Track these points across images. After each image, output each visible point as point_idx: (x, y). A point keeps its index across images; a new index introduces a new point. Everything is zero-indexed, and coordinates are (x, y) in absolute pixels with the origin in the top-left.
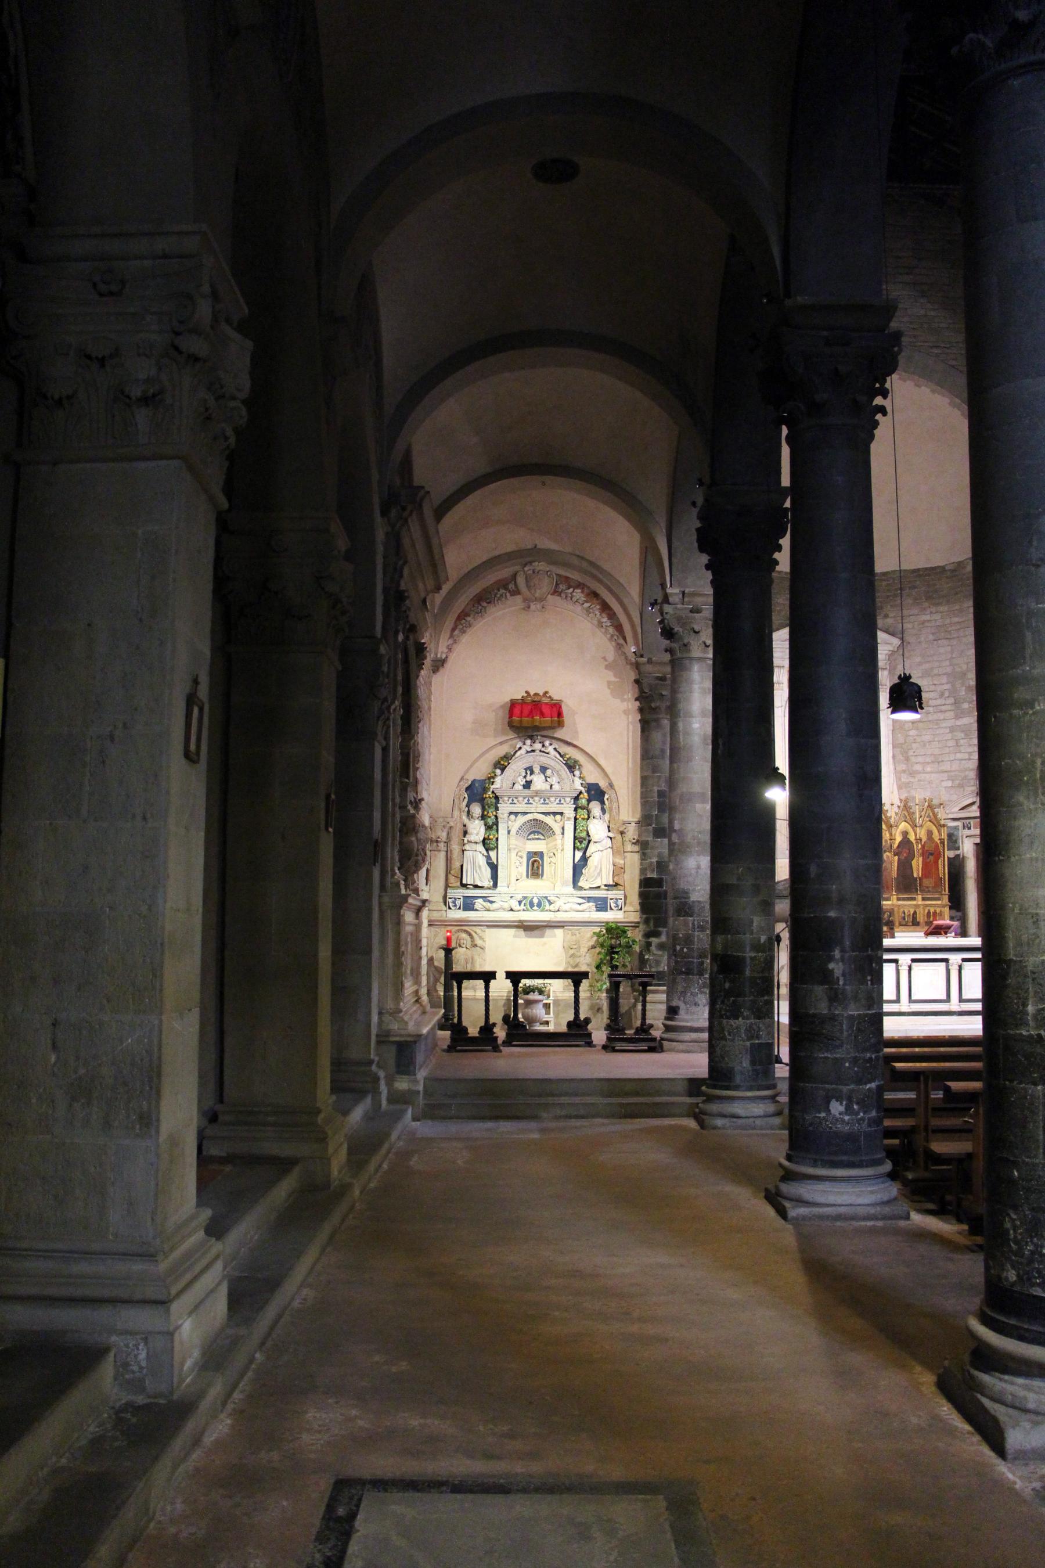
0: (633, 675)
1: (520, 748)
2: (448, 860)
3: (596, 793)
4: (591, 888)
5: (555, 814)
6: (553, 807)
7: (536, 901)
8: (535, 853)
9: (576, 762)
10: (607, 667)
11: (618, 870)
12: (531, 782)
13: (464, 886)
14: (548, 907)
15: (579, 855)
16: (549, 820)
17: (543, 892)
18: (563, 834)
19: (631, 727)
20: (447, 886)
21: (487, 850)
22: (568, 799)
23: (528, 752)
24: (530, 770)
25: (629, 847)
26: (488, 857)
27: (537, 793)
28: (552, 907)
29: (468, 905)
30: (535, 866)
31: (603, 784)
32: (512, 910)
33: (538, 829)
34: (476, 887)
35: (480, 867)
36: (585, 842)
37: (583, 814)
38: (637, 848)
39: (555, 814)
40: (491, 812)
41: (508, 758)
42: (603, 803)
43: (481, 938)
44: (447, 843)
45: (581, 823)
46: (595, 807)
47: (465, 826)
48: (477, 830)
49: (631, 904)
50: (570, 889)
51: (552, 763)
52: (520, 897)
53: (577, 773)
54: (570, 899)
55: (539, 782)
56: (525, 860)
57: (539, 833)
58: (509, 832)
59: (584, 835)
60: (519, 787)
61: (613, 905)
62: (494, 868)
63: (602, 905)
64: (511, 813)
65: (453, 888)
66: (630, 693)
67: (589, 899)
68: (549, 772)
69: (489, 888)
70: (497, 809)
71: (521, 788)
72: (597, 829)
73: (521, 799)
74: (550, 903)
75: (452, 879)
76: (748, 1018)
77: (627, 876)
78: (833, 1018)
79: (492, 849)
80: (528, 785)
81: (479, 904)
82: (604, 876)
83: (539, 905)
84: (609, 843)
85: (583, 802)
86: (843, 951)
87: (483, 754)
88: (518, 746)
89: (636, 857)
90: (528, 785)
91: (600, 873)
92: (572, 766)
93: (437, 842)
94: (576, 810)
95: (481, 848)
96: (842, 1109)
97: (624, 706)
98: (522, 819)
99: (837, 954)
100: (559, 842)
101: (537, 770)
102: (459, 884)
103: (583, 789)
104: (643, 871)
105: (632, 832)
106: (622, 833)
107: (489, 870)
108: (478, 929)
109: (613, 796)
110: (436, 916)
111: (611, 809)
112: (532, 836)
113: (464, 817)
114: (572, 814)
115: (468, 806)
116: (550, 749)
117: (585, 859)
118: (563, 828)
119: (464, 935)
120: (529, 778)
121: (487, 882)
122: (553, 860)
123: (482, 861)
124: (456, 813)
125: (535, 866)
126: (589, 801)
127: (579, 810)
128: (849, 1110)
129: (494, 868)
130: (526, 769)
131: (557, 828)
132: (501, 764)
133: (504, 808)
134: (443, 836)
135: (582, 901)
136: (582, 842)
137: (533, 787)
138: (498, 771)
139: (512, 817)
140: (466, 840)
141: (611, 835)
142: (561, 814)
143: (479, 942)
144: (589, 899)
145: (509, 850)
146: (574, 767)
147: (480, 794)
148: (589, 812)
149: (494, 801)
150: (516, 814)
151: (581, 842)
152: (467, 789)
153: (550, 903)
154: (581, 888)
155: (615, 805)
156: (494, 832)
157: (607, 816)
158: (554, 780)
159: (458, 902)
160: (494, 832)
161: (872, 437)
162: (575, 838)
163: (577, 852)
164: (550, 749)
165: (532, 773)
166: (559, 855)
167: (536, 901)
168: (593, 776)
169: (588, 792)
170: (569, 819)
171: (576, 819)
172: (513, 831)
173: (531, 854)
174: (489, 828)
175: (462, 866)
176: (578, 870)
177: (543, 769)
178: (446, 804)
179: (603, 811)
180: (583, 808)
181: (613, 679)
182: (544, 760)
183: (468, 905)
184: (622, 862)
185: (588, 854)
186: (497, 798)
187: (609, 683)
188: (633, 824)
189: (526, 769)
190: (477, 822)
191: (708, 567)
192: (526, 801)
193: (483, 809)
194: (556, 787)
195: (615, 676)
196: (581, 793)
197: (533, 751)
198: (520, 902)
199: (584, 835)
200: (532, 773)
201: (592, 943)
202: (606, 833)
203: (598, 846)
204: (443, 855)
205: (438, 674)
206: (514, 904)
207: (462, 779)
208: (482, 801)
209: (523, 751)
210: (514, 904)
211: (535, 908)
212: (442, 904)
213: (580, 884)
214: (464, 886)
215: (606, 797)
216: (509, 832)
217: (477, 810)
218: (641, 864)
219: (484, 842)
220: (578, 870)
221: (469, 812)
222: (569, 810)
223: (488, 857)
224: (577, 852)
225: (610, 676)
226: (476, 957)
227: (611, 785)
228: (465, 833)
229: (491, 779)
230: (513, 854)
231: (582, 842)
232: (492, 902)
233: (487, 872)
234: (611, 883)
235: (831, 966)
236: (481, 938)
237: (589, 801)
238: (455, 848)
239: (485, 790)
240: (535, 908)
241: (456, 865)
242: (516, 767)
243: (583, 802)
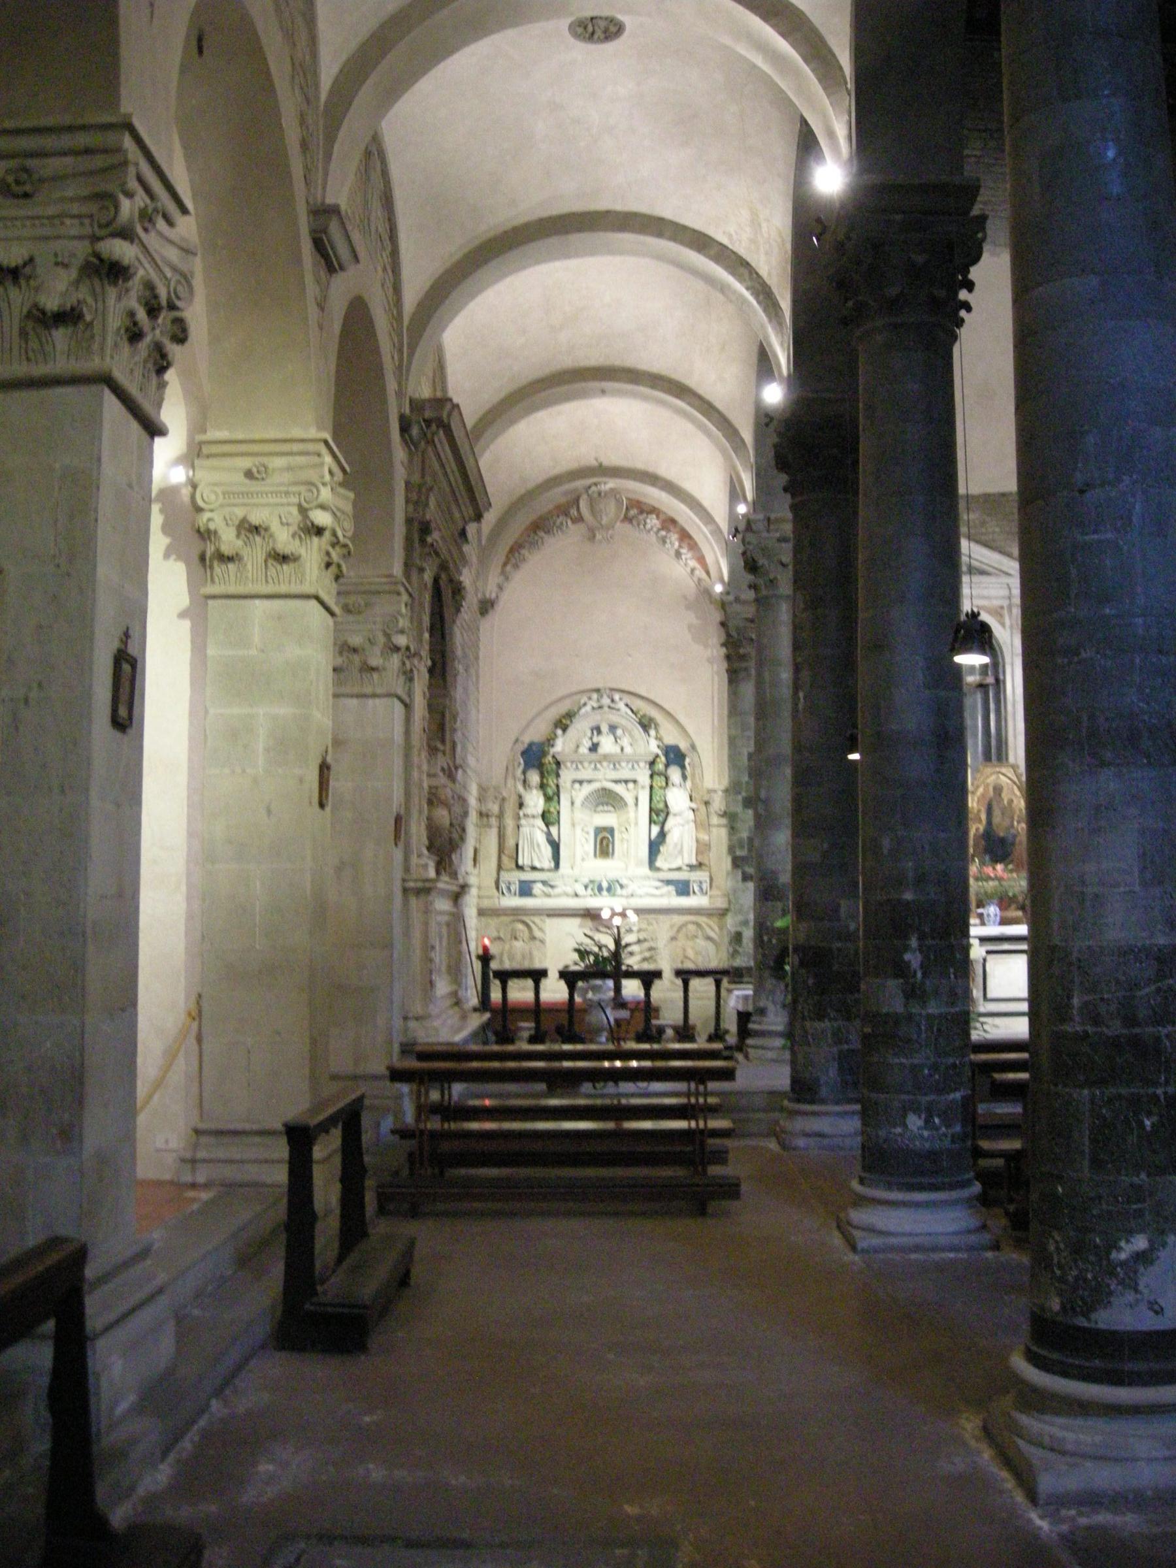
0: (717, 616)
1: (585, 704)
2: (501, 837)
3: (675, 756)
4: (671, 870)
6: (625, 773)
7: (605, 885)
8: (604, 829)
9: (651, 720)
10: (688, 608)
11: (702, 848)
13: (520, 868)
14: (619, 891)
15: (655, 830)
17: (612, 875)
18: (636, 804)
19: (716, 678)
20: (500, 868)
21: (547, 825)
22: (642, 764)
23: (593, 708)
24: (598, 730)
25: (715, 820)
26: (549, 834)
27: (606, 757)
28: (624, 892)
29: (525, 890)
30: (604, 843)
31: (683, 746)
32: (576, 895)
33: (607, 799)
34: (534, 868)
35: (538, 845)
36: (663, 815)
37: (659, 781)
38: (724, 821)
39: (626, 782)
40: (551, 781)
41: (570, 715)
42: (683, 767)
43: (541, 929)
44: (501, 816)
45: (658, 792)
46: (675, 774)
47: (520, 797)
48: (535, 802)
49: (718, 888)
50: (645, 870)
51: (623, 722)
52: (586, 880)
53: (652, 732)
54: (647, 883)
55: (607, 744)
57: (607, 804)
58: (573, 803)
59: (661, 806)
60: (584, 750)
61: (696, 889)
62: (555, 846)
63: (683, 889)
64: (574, 781)
65: (508, 870)
66: (715, 637)
67: (668, 882)
68: (619, 732)
69: (549, 870)
70: (558, 776)
72: (677, 798)
73: (586, 764)
74: (622, 886)
75: (506, 861)
76: (836, 1020)
77: (713, 855)
78: (910, 1017)
79: (553, 824)
80: (594, 748)
81: (538, 888)
82: (686, 855)
83: (609, 889)
84: (691, 815)
85: (660, 766)
86: (921, 938)
87: (539, 714)
88: (582, 702)
89: (723, 833)
90: (594, 748)
91: (681, 852)
92: (646, 724)
93: (488, 816)
94: (651, 776)
95: (540, 823)
96: (920, 1123)
97: (709, 653)
98: (587, 789)
99: (914, 942)
100: (632, 814)
101: (605, 728)
102: (514, 866)
103: (660, 752)
104: (731, 850)
105: (718, 803)
106: (707, 803)
107: (549, 849)
108: (537, 919)
109: (696, 759)
110: (486, 903)
111: (693, 775)
112: (601, 808)
113: (520, 788)
114: (647, 782)
115: (524, 773)
116: (621, 705)
117: (662, 835)
118: (637, 799)
119: (520, 926)
120: (595, 740)
121: (546, 861)
122: (625, 836)
123: (541, 838)
124: (510, 782)
125: (604, 843)
126: (667, 766)
127: (656, 777)
128: (928, 1122)
129: (555, 846)
131: (629, 798)
132: (563, 723)
133: (567, 776)
134: (495, 809)
135: (659, 884)
136: (659, 814)
137: (601, 750)
138: (559, 732)
139: (577, 786)
140: (521, 813)
141: (694, 805)
142: (635, 782)
143: (537, 933)
144: (668, 882)
145: (573, 825)
146: (650, 726)
147: (537, 759)
148: (667, 779)
150: (581, 782)
151: (657, 815)
152: (523, 753)
153: (622, 886)
154: (658, 869)
155: (698, 771)
157: (689, 783)
158: (625, 742)
159: (513, 888)
160: (554, 803)
161: (954, 338)
162: (651, 809)
163: (653, 826)
164: (621, 705)
166: (632, 829)
167: (605, 885)
168: (672, 737)
169: (666, 755)
170: (643, 787)
171: (651, 787)
172: (578, 803)
173: (599, 830)
174: (548, 799)
175: (517, 845)
176: (654, 847)
177: (613, 728)
178: (498, 771)
179: (684, 777)
180: (660, 774)
181: (695, 622)
182: (614, 718)
183: (525, 890)
184: (706, 838)
185: (666, 828)
186: (558, 764)
187: (690, 627)
188: (720, 793)
190: (535, 792)
191: (785, 490)
193: (542, 776)
194: (628, 750)
195: (697, 618)
197: (600, 707)
198: (586, 887)
199: (661, 806)
200: (599, 732)
201: (672, 934)
202: (688, 803)
203: (679, 820)
204: (494, 832)
205: (489, 617)
206: (580, 890)
207: (517, 740)
208: (540, 767)
209: (588, 708)
210: (580, 890)
211: (605, 893)
212: (495, 891)
213: (658, 864)
214: (520, 868)
215: (687, 761)
216: (573, 803)
217: (534, 778)
218: (730, 840)
219: (544, 816)
220: (654, 847)
221: (525, 781)
222: (643, 776)
223: (549, 834)
224: (653, 826)
225: (691, 618)
226: (535, 953)
227: (693, 747)
228: (521, 805)
229: (550, 741)
230: (578, 831)
231: (659, 814)
232: (552, 887)
233: (547, 851)
234: (694, 862)
235: (907, 957)
236: (541, 929)
237: (667, 766)
238: (509, 822)
239: (544, 754)
240: (605, 893)
241: (510, 842)
242: (580, 728)
243: (660, 766)
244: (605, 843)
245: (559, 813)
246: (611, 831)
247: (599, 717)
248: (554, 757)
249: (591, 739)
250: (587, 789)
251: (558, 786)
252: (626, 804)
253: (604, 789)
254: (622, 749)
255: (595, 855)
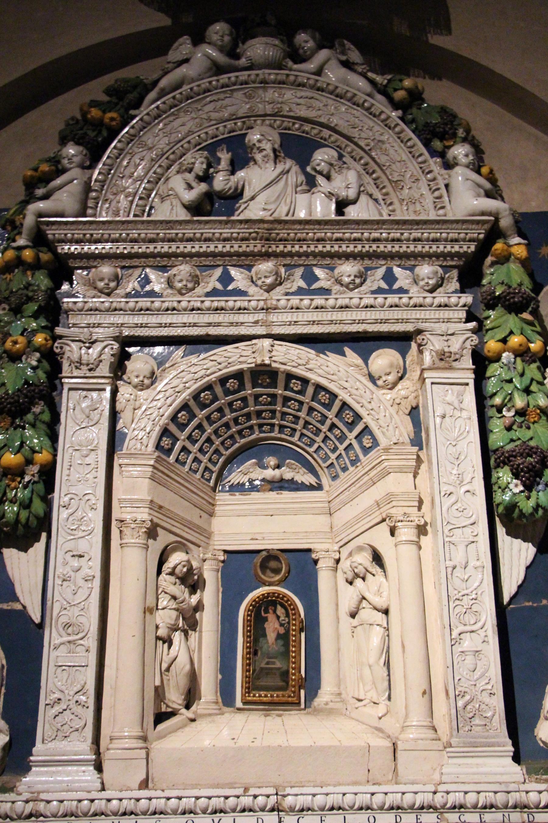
5: (364, 342)
6: (357, 307)
8: (269, 560)
12: (237, 195)
16: (337, 371)
39: (364, 342)
51: (341, 116)
56: (210, 596)
57: (284, 454)
71: (183, 215)
130: (212, 149)
149: (42, 281)
156: (34, 439)
162: (490, 459)
165: (241, 159)
170: (444, 359)
171: (481, 362)
173: (242, 567)
177: (296, 148)
180: (515, 303)
189: (212, 149)
192: (212, 281)
196: (495, 233)
244: (272, 628)
245: (48, 474)
246: (298, 566)
247: (237, 103)
248: (40, 239)
249: (206, 178)
250: (188, 372)
251: (52, 362)
252: (367, 437)
253: (264, 374)
254: (342, 206)
255: (226, 696)
